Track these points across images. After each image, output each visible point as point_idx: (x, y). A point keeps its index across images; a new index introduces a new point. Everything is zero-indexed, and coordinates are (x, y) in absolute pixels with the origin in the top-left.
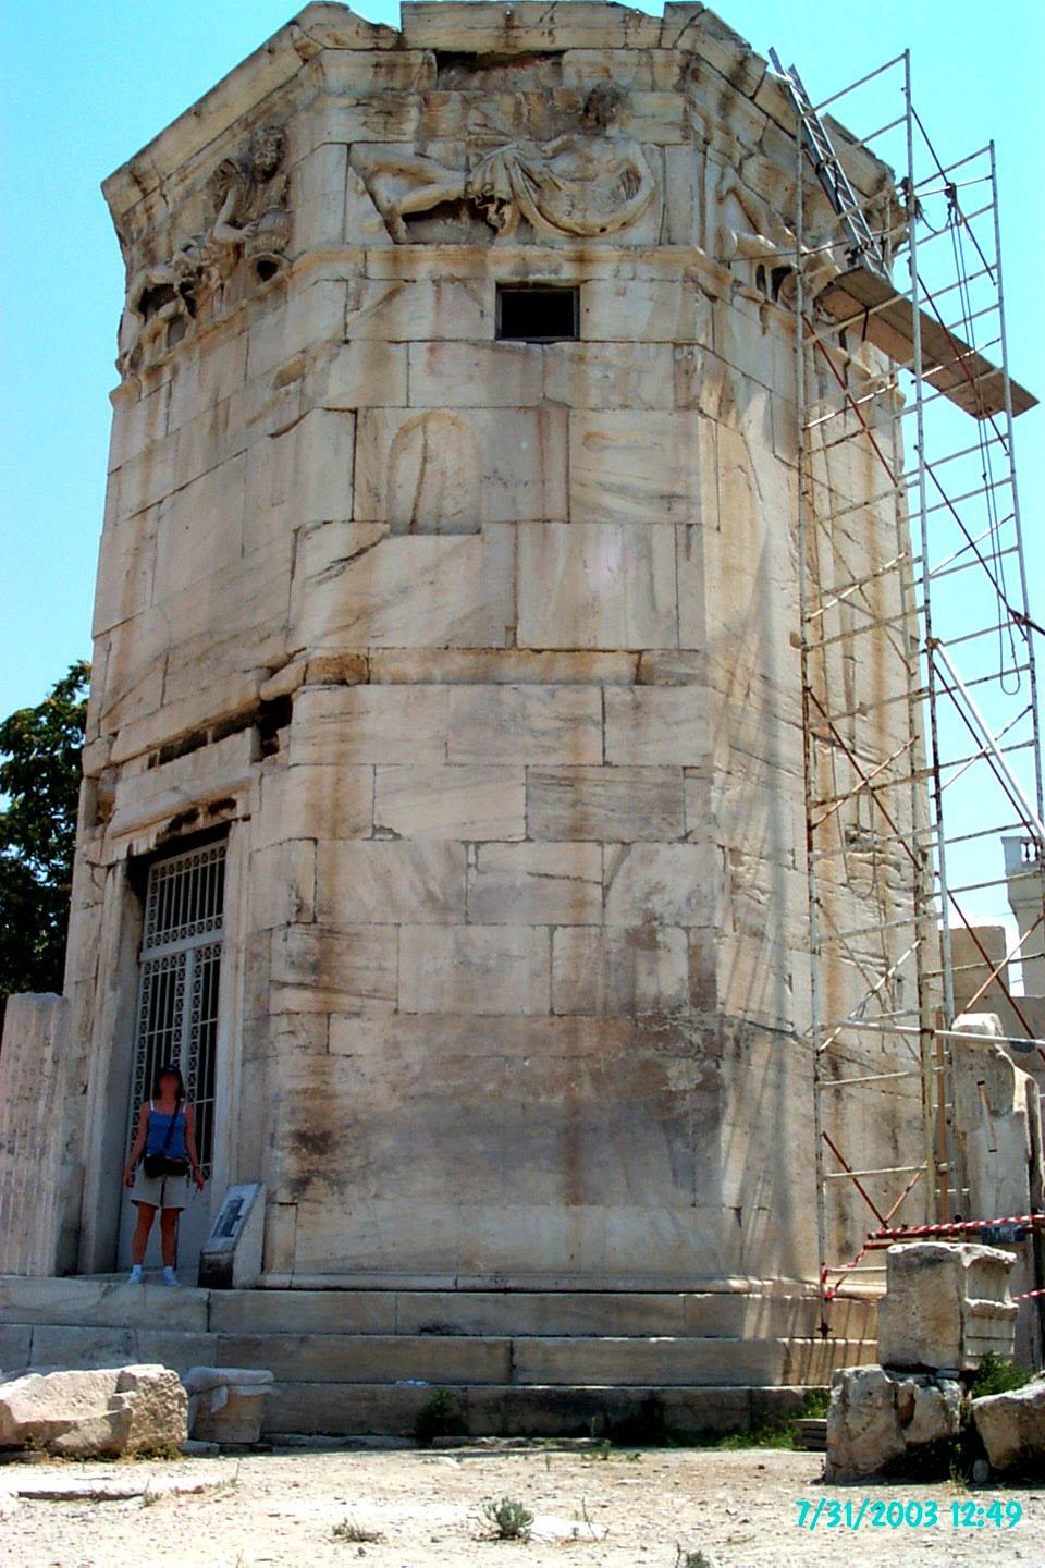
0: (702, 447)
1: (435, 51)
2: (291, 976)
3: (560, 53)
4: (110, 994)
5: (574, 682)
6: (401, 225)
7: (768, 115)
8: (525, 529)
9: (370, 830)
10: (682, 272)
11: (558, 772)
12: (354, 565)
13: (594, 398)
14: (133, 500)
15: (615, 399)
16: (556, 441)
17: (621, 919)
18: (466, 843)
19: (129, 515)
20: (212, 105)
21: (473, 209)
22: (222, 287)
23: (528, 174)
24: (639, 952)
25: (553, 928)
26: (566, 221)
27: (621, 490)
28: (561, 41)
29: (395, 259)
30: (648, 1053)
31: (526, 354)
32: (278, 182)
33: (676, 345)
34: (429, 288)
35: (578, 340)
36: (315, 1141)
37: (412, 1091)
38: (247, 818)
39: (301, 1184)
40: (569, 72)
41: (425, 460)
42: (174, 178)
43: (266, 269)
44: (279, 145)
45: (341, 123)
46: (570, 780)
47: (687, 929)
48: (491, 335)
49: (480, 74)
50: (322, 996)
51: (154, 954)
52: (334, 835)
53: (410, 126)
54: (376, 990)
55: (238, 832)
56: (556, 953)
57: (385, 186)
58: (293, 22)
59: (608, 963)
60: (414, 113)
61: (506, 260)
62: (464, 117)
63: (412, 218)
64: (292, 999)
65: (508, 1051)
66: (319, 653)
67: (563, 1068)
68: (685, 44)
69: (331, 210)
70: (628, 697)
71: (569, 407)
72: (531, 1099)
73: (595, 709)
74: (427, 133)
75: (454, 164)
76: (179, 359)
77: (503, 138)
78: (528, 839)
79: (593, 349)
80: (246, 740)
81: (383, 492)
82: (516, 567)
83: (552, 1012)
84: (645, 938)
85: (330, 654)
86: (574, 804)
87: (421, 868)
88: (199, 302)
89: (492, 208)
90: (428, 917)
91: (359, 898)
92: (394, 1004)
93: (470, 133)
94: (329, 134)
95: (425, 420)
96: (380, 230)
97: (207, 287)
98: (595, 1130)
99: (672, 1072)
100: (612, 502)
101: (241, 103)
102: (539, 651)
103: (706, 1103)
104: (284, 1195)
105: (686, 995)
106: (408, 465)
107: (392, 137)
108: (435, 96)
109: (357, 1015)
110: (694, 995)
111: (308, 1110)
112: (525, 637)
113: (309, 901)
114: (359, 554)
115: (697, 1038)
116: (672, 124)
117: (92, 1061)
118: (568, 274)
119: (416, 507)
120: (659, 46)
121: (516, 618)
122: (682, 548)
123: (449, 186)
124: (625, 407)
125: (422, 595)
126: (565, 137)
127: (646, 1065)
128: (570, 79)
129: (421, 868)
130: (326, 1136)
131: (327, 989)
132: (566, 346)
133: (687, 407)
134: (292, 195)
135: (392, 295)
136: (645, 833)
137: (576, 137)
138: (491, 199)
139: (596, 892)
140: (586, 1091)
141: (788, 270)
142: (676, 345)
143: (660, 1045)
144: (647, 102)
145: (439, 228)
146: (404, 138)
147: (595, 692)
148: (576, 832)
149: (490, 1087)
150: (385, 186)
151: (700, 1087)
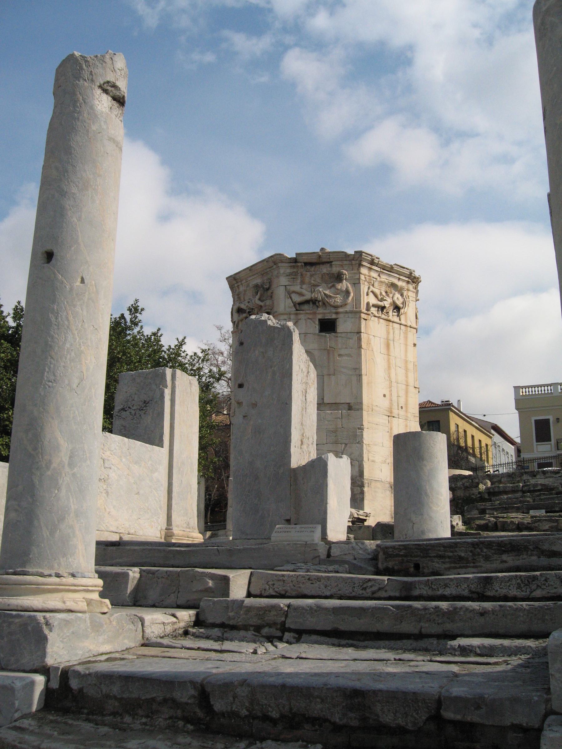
3: (331, 262)
6: (298, 306)
11: (332, 430)
13: (340, 346)
21: (313, 302)
28: (331, 260)
32: (270, 291)
34: (304, 322)
42: (244, 281)
44: (270, 283)
45: (283, 281)
46: (335, 431)
48: (317, 332)
53: (299, 281)
60: (299, 279)
62: (310, 279)
63: (301, 304)
73: (340, 416)
79: (339, 335)
82: (323, 386)
100: (342, 370)
118: (334, 316)
123: (308, 296)
124: (346, 348)
145: (306, 307)
148: (336, 442)
150: (294, 296)
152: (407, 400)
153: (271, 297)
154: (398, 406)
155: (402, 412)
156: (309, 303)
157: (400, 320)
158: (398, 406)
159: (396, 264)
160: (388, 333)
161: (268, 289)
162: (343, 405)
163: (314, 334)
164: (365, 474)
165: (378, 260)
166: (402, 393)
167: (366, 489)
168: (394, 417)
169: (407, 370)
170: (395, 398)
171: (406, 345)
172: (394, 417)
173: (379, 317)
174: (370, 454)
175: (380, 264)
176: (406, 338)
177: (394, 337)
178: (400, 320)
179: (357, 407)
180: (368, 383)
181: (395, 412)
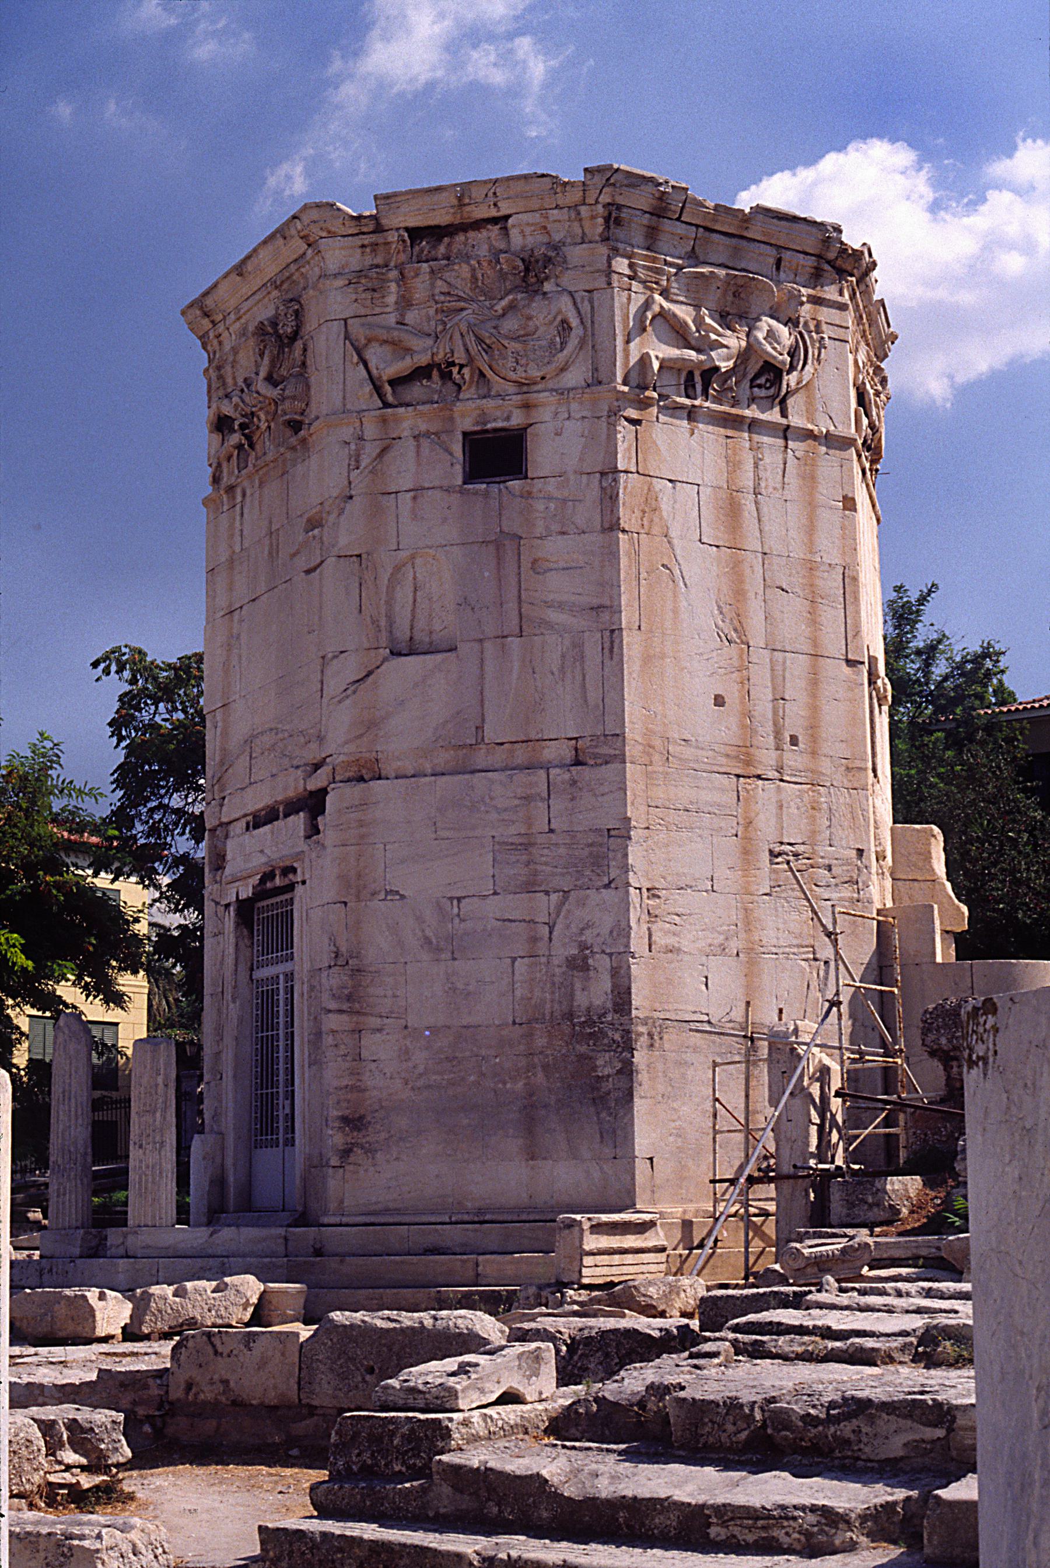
0: (624, 561)
1: (407, 229)
2: (333, 1005)
3: (507, 217)
4: (232, 1006)
5: (529, 767)
7: (697, 226)
8: (487, 645)
9: (383, 893)
10: (607, 408)
13: (539, 530)
14: (222, 601)
15: (555, 527)
16: (510, 568)
17: (563, 950)
18: (451, 899)
19: (222, 613)
20: (250, 267)
22: (269, 427)
23: (480, 340)
24: (575, 973)
25: (514, 960)
26: (513, 376)
27: (561, 606)
28: (504, 212)
29: (384, 420)
30: (582, 1049)
31: (486, 494)
32: (299, 345)
33: (603, 474)
34: (412, 442)
35: (526, 477)
36: (353, 1122)
37: (420, 1083)
38: (304, 882)
39: (346, 1153)
40: (514, 233)
41: (416, 590)
42: (233, 316)
43: (295, 426)
44: (297, 313)
47: (611, 955)
48: (459, 481)
49: (446, 240)
51: (261, 973)
52: (358, 899)
53: (391, 299)
54: (392, 1012)
55: (299, 889)
56: (517, 977)
57: (375, 355)
58: (294, 217)
59: (554, 984)
60: (393, 287)
61: (468, 413)
62: (433, 286)
64: (332, 1022)
65: (483, 1052)
66: (342, 758)
67: (523, 1062)
68: (605, 198)
69: (335, 382)
70: (567, 776)
71: (521, 538)
74: (405, 303)
75: (426, 329)
76: (246, 483)
77: (462, 304)
78: (495, 893)
79: (539, 484)
80: (299, 820)
81: (383, 623)
82: (482, 677)
83: (514, 1023)
84: (579, 964)
86: (528, 864)
87: (420, 919)
88: (255, 439)
89: (455, 370)
90: (425, 956)
91: (378, 945)
93: (437, 303)
94: (332, 306)
95: (413, 557)
96: (371, 396)
97: (258, 427)
98: (545, 1106)
100: (554, 616)
101: (269, 266)
102: (502, 744)
103: (623, 1084)
104: (334, 1161)
105: (609, 1005)
106: (404, 595)
107: (377, 310)
108: (409, 272)
109: (379, 1031)
110: (615, 1004)
111: (349, 1101)
112: (490, 733)
113: (343, 949)
114: (367, 676)
115: (617, 1037)
116: (598, 271)
117: (224, 1056)
118: (517, 420)
119: (412, 629)
120: (584, 204)
121: (483, 720)
122: (606, 651)
125: (416, 704)
126: (511, 297)
127: (581, 1057)
128: (516, 239)
129: (420, 919)
130: (361, 1118)
132: (515, 484)
133: (611, 529)
134: (308, 362)
135: (384, 451)
137: (519, 296)
138: (453, 364)
140: (540, 1078)
142: (603, 474)
143: (591, 1043)
144: (576, 254)
145: (416, 391)
146: (388, 310)
147: (542, 773)
148: (530, 887)
149: (472, 1078)
151: (620, 1072)
152: (814, 710)
153: (304, 364)
155: (794, 759)
156: (429, 377)
157: (784, 414)
158: (778, 734)
160: (733, 465)
161: (295, 336)
164: (637, 1000)
166: (796, 688)
167: (640, 1058)
168: (759, 777)
170: (763, 707)
171: (812, 506)
173: (691, 414)
176: (810, 479)
177: (758, 479)
178: (784, 414)
179: (605, 750)
180: (647, 659)
181: (766, 758)
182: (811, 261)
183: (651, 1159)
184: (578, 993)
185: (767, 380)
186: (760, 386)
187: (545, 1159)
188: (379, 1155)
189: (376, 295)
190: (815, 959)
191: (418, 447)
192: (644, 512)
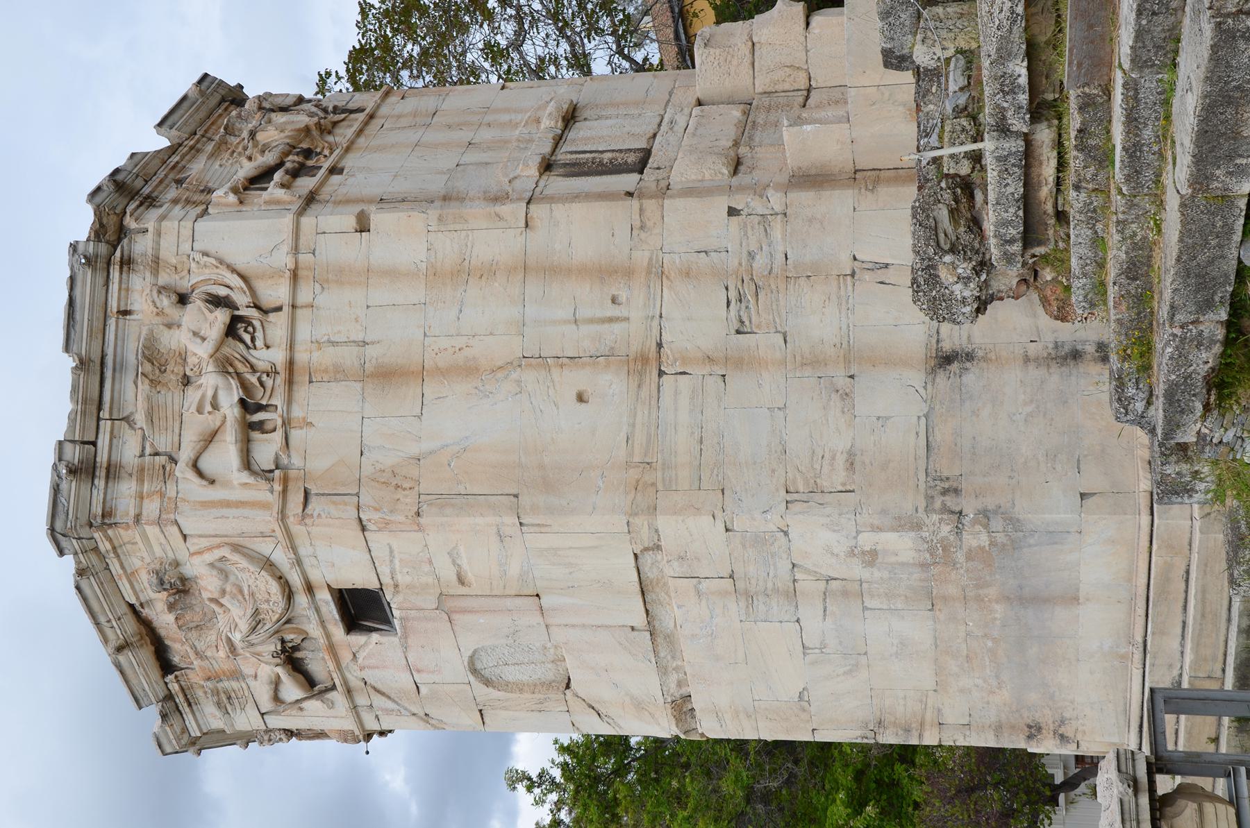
1: (164, 676)
12: (602, 711)
13: (431, 580)
25: (865, 608)
28: (125, 609)
36: (1034, 731)
37: (995, 683)
48: (395, 640)
50: (927, 727)
53: (235, 685)
54: (921, 701)
56: (885, 607)
72: (998, 622)
78: (798, 621)
79: (386, 580)
85: (674, 722)
92: (931, 693)
99: (974, 543)
100: (514, 569)
105: (912, 534)
110: (912, 529)
118: (324, 596)
122: (543, 530)
124: (430, 562)
127: (969, 558)
130: (1030, 727)
131: (922, 724)
136: (785, 556)
139: (834, 584)
140: (992, 592)
141: (242, 402)
142: (364, 529)
154: (611, 320)
157: (279, 309)
158: (611, 320)
159: (67, 348)
162: (646, 569)
163: (406, 648)
165: (68, 448)
168: (660, 345)
169: (463, 273)
172: (660, 345)
174: (825, 483)
175: (83, 429)
178: (279, 309)
182: (115, 273)
183: (1083, 496)
184: (901, 559)
185: (246, 331)
186: (253, 339)
187: (1078, 590)
188: (1067, 715)
189: (233, 695)
190: (853, 275)
191: (369, 667)
192: (397, 486)
